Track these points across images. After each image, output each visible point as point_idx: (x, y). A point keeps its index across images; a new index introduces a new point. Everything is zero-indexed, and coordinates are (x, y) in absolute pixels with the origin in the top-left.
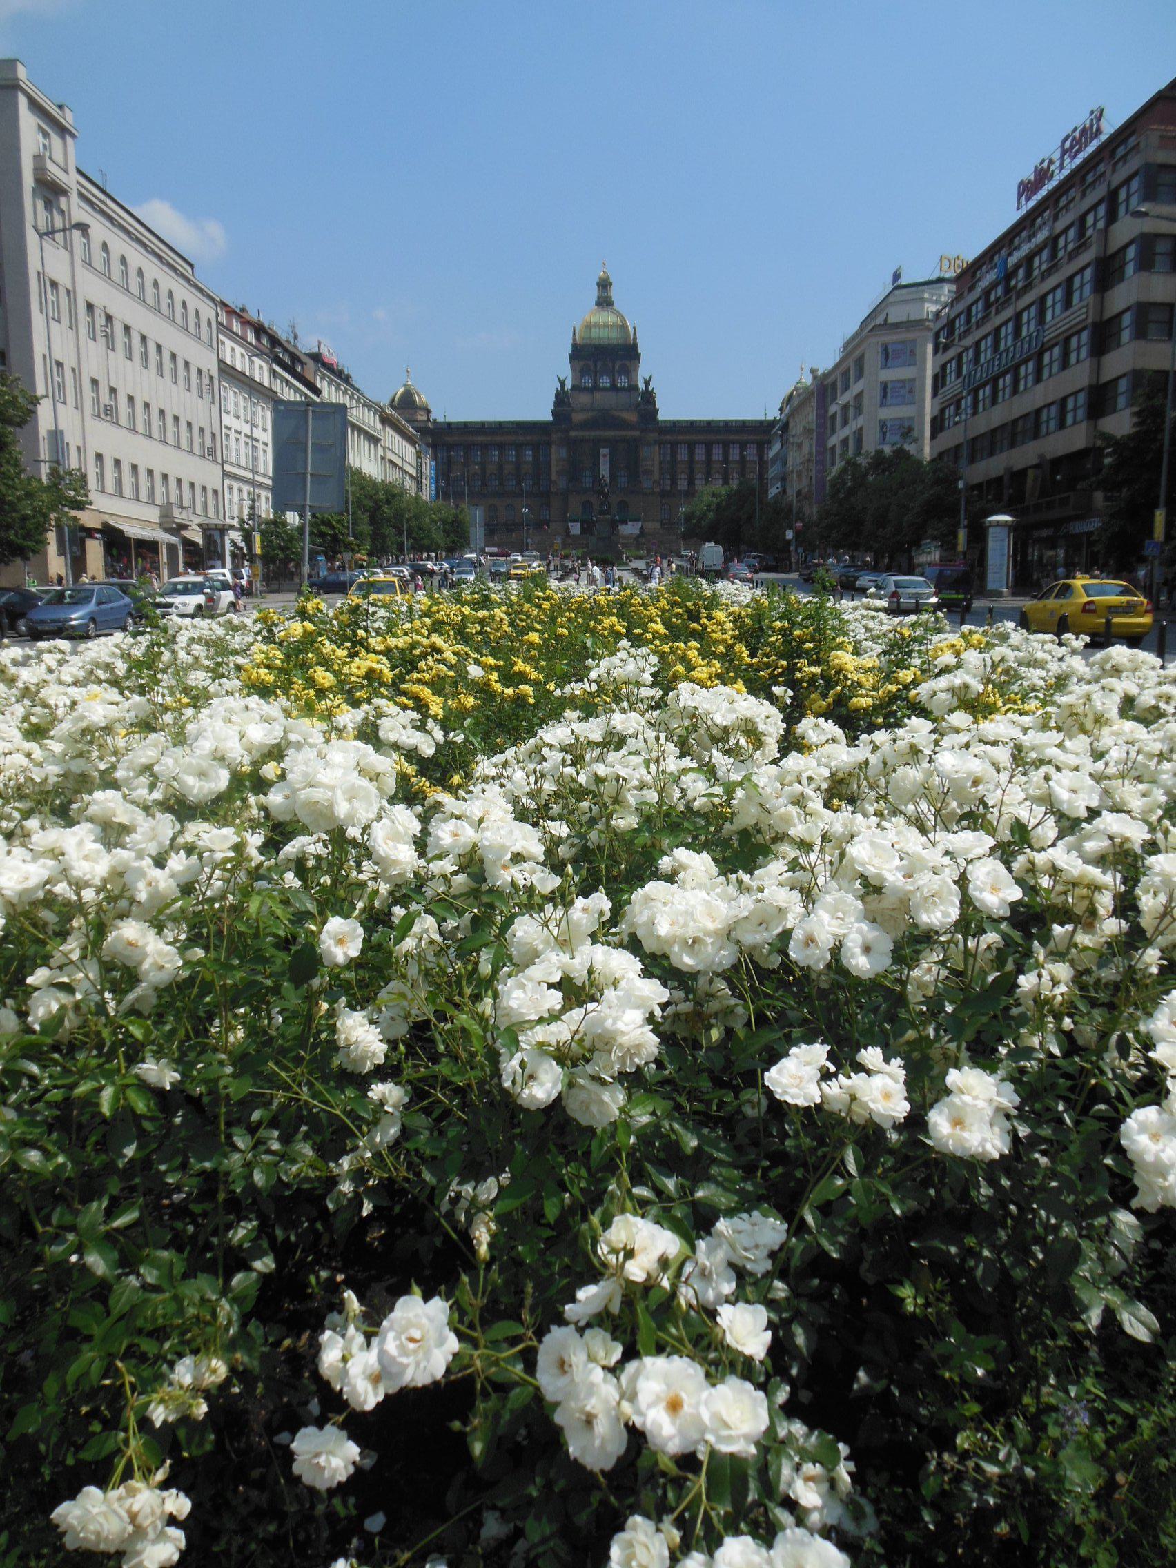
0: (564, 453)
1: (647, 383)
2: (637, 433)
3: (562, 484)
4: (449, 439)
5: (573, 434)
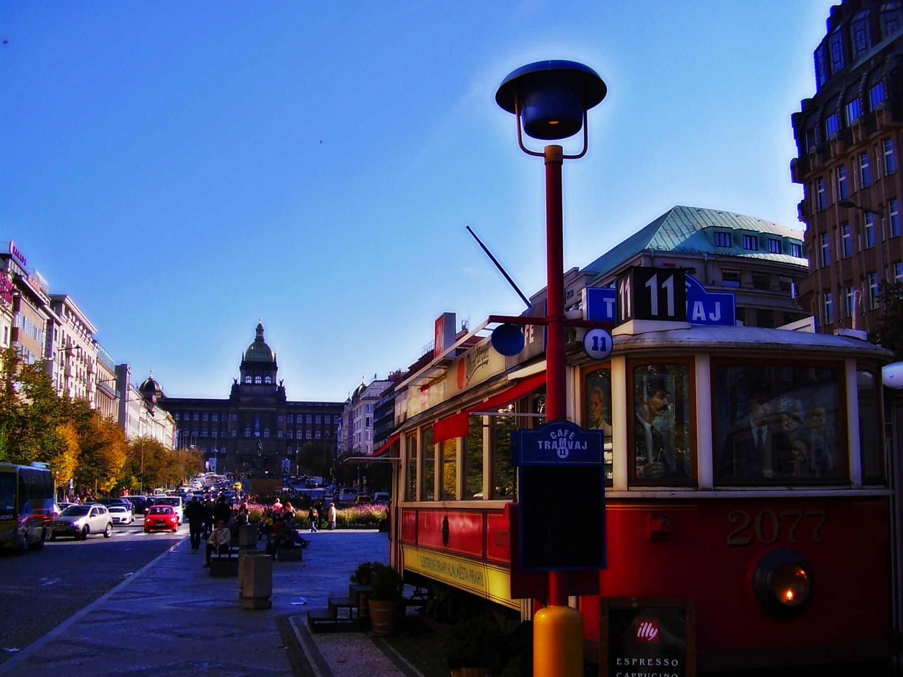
0: (235, 417)
1: (281, 383)
2: (275, 409)
3: (234, 435)
5: (240, 408)
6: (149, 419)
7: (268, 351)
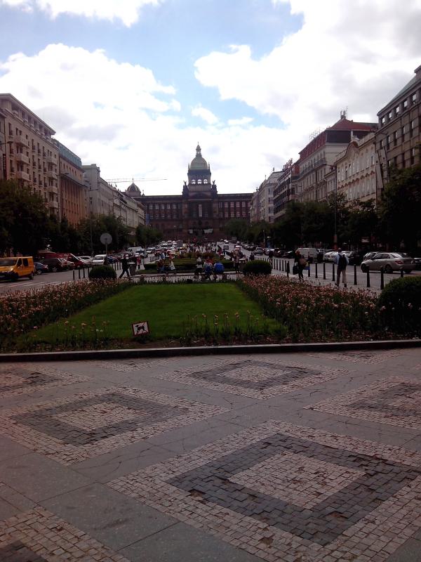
0: (186, 206)
1: (214, 182)
4: (148, 202)
6: (123, 206)
7: (204, 163)
